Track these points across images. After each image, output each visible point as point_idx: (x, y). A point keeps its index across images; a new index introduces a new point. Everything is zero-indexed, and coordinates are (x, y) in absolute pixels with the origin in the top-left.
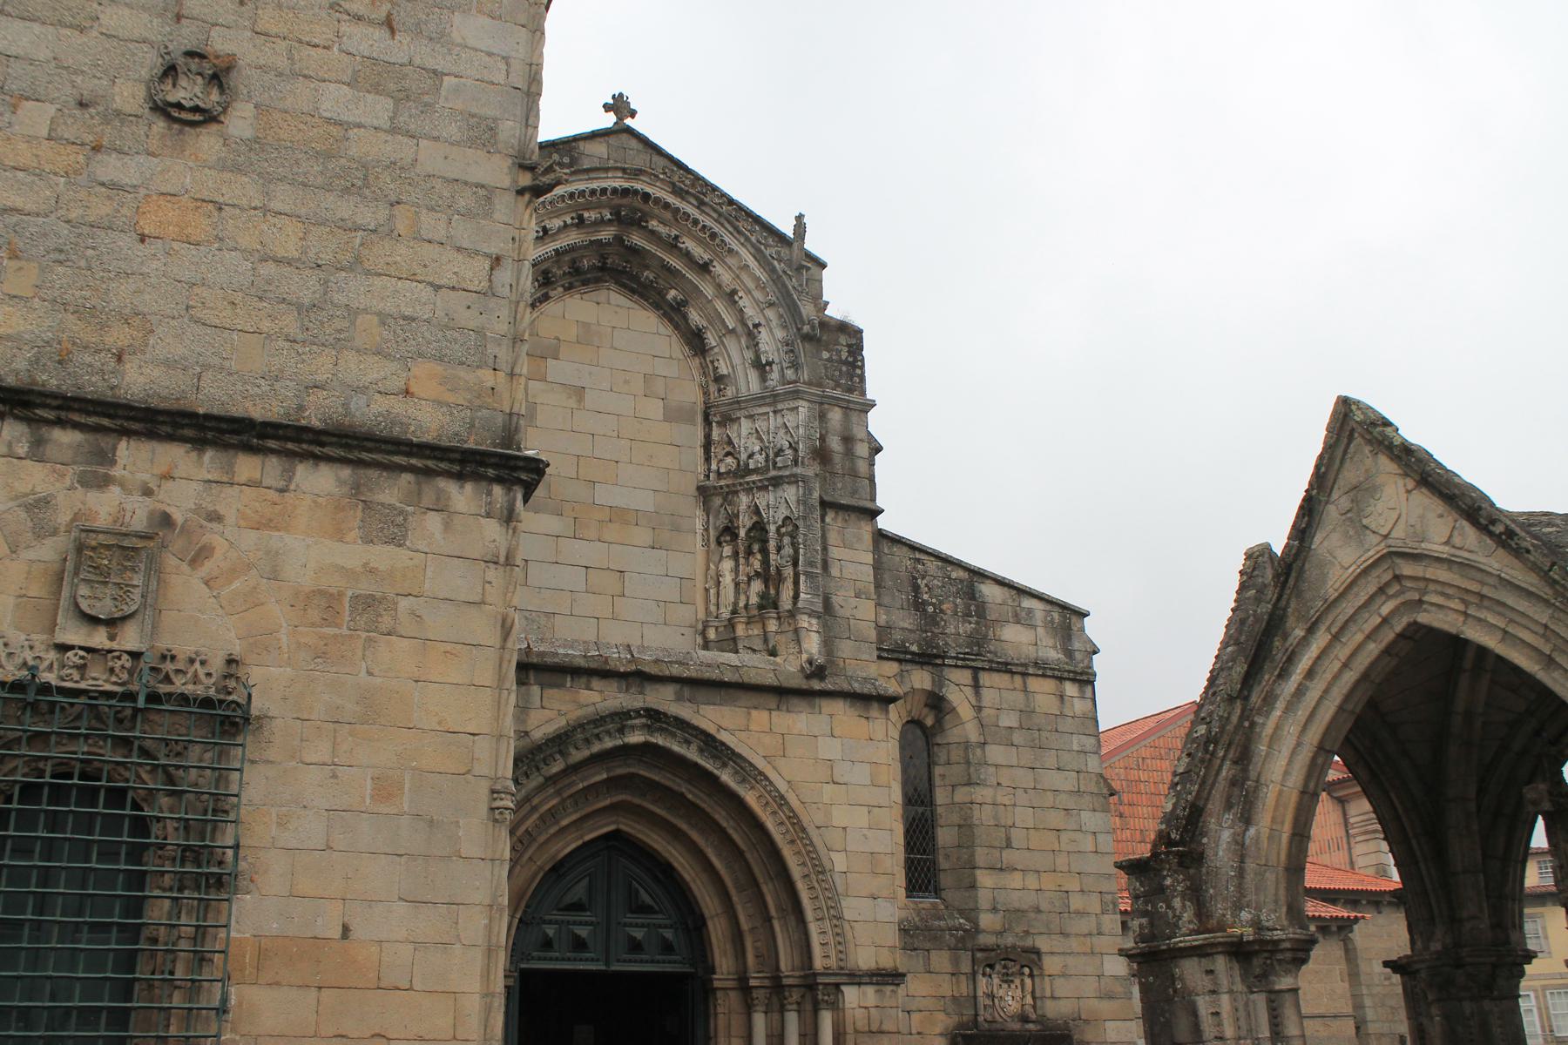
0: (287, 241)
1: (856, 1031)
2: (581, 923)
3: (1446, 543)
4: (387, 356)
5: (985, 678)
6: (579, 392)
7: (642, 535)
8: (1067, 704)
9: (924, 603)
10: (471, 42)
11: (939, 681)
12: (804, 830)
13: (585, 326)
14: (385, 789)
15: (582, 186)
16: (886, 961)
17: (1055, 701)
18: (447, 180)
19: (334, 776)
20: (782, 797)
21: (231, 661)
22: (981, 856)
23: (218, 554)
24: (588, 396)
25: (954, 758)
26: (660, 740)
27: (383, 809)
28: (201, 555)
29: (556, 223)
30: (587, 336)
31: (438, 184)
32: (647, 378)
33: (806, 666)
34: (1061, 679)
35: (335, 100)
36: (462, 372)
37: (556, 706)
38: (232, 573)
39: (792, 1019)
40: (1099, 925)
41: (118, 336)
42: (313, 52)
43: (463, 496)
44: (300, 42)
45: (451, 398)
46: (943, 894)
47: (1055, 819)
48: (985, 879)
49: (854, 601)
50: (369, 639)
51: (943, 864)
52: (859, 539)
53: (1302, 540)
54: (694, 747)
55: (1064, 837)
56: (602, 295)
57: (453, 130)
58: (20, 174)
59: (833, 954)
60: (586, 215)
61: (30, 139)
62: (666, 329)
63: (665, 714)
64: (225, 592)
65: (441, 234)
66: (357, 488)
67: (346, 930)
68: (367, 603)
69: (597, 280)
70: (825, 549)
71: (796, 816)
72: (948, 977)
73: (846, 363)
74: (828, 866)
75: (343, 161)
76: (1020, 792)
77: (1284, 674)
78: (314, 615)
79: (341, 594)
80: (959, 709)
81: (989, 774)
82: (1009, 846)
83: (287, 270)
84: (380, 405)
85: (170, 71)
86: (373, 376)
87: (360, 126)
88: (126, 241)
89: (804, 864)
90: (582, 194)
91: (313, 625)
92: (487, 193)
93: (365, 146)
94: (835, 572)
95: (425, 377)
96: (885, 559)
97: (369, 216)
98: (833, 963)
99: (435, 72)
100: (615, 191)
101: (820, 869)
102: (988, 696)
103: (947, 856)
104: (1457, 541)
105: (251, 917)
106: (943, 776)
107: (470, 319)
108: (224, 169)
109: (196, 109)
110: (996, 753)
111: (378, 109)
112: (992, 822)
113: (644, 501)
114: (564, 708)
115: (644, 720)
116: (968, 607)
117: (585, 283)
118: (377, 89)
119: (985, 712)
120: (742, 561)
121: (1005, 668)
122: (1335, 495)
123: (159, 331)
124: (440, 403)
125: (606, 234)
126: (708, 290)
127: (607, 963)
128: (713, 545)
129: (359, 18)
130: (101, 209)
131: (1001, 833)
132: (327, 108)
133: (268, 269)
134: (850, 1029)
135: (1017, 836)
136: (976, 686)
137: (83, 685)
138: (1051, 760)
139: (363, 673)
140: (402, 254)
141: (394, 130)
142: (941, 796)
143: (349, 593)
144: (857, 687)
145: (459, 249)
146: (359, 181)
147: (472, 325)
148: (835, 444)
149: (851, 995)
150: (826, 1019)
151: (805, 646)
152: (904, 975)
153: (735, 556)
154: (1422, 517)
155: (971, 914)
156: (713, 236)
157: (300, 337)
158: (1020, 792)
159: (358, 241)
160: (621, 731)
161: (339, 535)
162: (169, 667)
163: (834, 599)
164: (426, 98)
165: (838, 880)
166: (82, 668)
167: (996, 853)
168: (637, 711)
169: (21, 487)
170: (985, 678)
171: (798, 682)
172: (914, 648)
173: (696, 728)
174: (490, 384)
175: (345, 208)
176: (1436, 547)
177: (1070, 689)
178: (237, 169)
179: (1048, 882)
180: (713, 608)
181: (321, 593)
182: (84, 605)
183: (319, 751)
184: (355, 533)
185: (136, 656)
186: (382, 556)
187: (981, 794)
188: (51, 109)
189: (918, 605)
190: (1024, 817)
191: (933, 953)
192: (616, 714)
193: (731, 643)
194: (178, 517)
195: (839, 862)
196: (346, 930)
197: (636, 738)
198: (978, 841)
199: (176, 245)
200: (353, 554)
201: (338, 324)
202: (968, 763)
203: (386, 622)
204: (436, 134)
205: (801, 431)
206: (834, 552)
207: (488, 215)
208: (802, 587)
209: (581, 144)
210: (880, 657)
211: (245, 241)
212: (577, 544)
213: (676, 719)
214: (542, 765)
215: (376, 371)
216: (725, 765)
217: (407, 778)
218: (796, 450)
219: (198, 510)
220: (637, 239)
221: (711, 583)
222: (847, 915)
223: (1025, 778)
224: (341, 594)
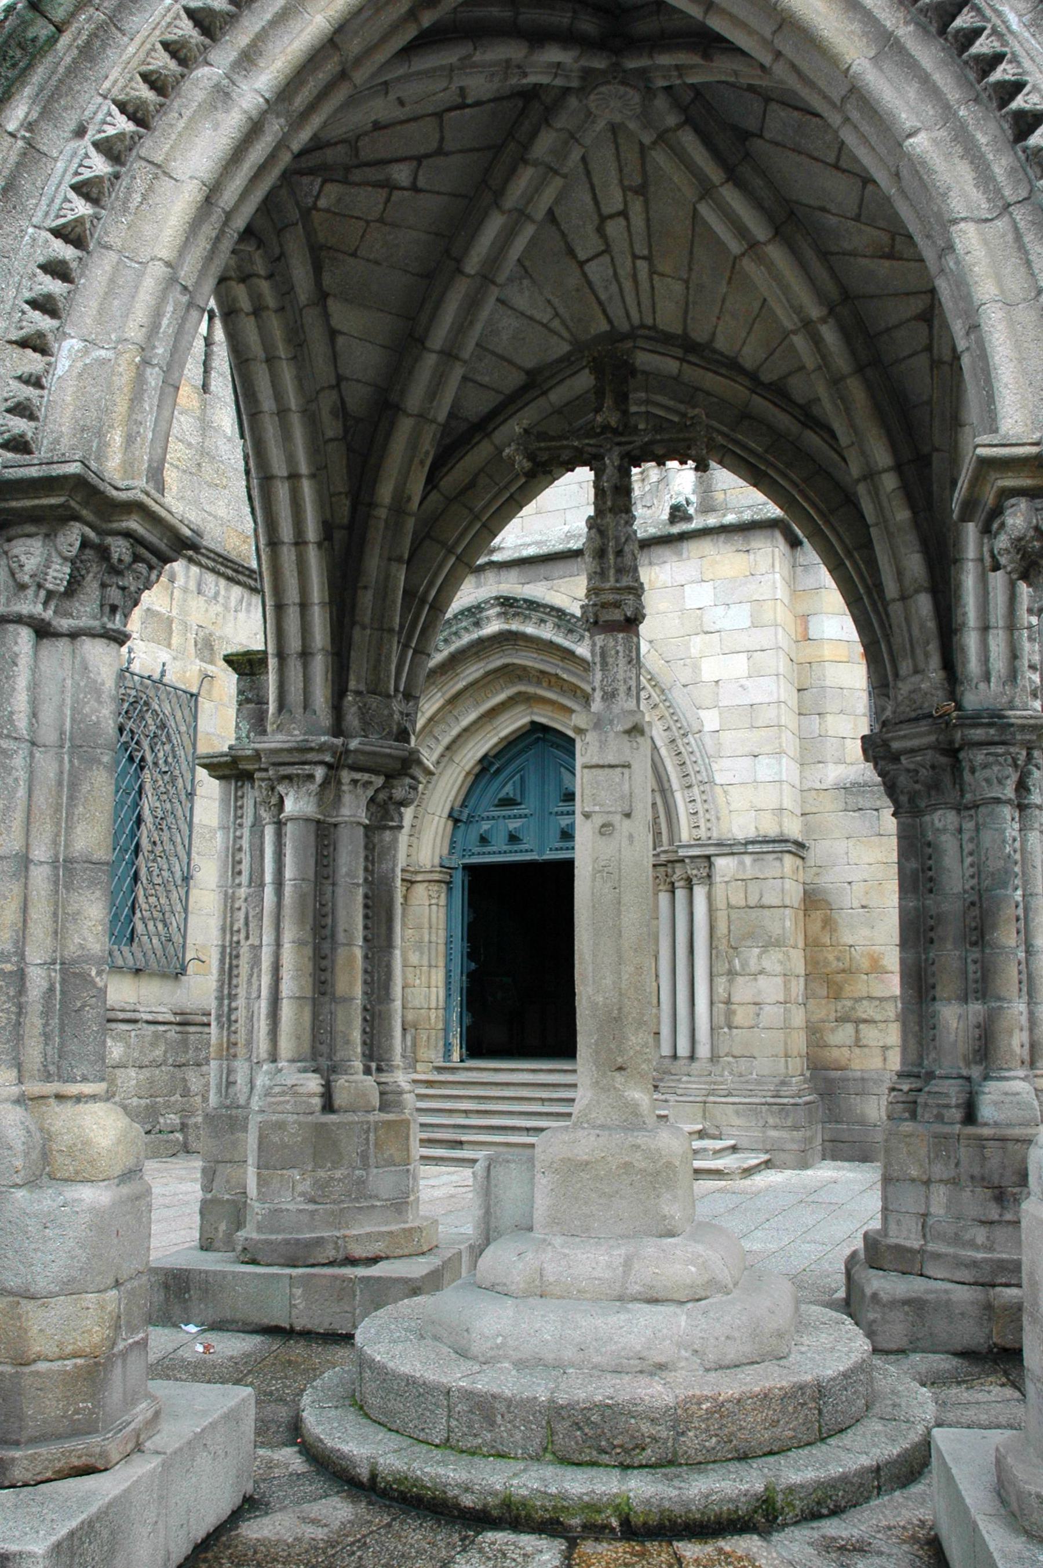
1: (729, 906)
12: (663, 691)
26: (515, 626)
39: (681, 894)
54: (550, 625)
63: (516, 600)
115: (498, 609)
127: (541, 853)
149: (724, 865)
150: (700, 893)
160: (477, 624)
165: (708, 740)
168: (486, 602)
173: (545, 606)
192: (469, 609)
195: (710, 720)
197: (493, 627)
213: (525, 601)
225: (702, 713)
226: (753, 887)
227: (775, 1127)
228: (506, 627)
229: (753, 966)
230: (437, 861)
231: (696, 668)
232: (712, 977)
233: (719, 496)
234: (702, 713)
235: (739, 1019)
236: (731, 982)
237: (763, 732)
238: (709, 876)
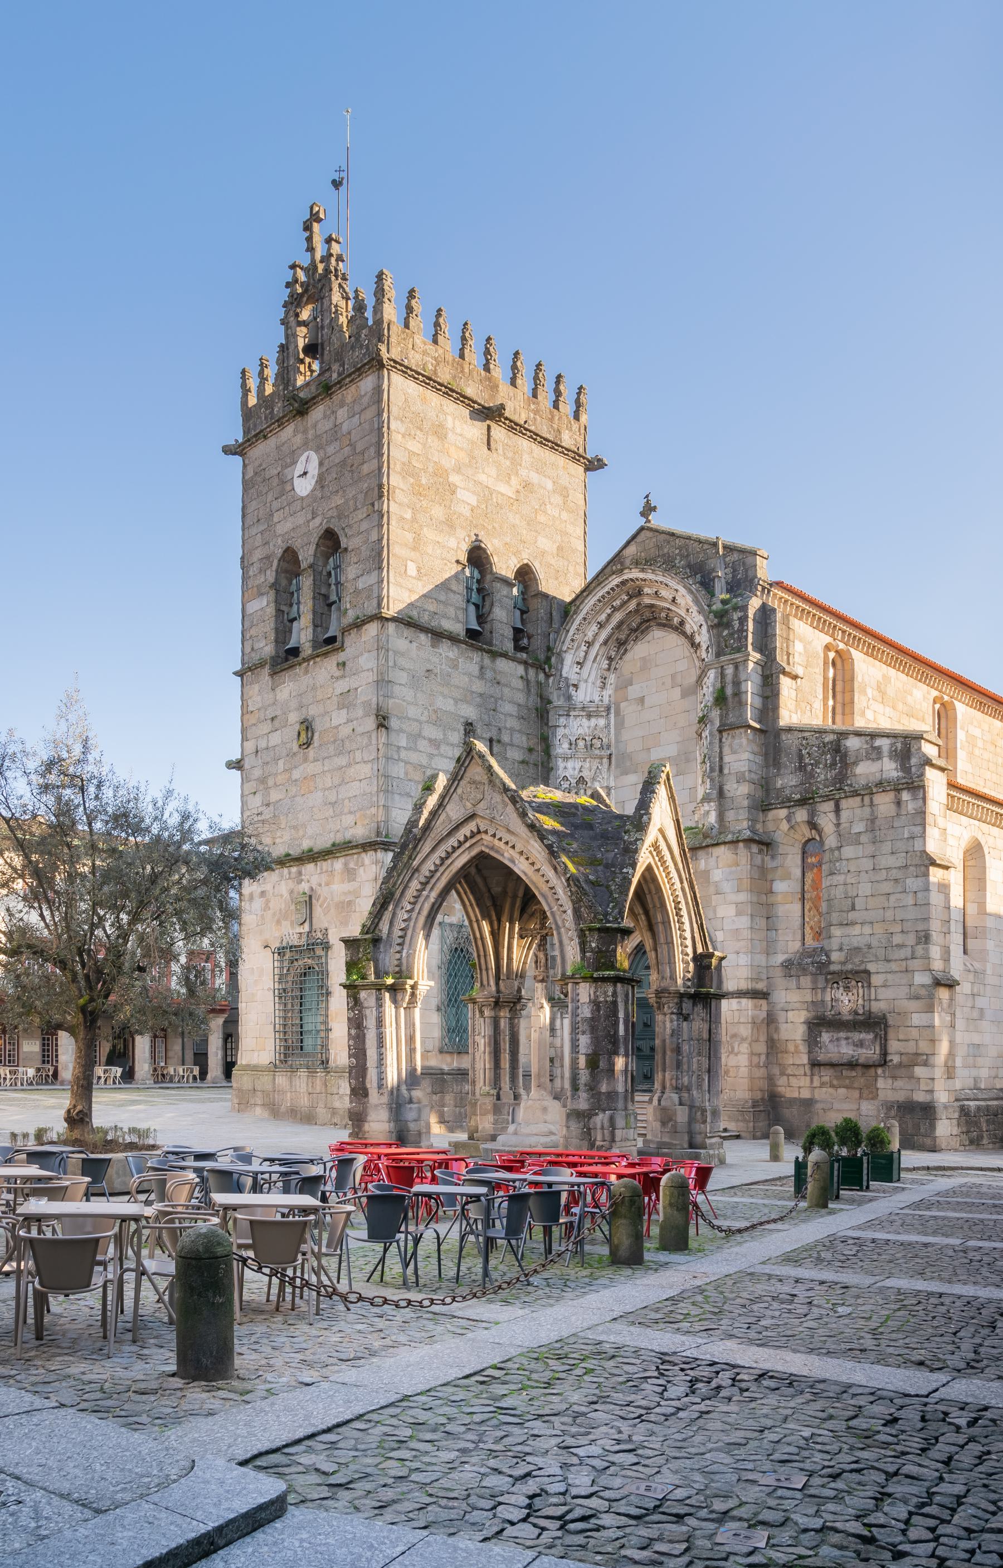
5: (844, 804)
6: (641, 700)
8: (903, 806)
11: (812, 814)
13: (643, 659)
15: (600, 594)
17: (893, 807)
29: (603, 617)
30: (646, 664)
32: (673, 676)
40: (913, 952)
47: (886, 887)
48: (837, 932)
52: (741, 746)
55: (892, 898)
56: (649, 637)
62: (681, 640)
69: (647, 628)
82: (853, 908)
90: (603, 597)
95: (348, 820)
97: (342, 761)
102: (844, 815)
107: (368, 790)
116: (834, 759)
117: (642, 632)
121: (855, 794)
125: (632, 605)
131: (849, 902)
132: (335, 722)
135: (859, 903)
138: (887, 847)
140: (351, 771)
148: (729, 691)
158: (863, 874)
167: (845, 915)
179: (879, 929)
190: (865, 889)
220: (647, 601)
223: (867, 864)
237: (743, 943)
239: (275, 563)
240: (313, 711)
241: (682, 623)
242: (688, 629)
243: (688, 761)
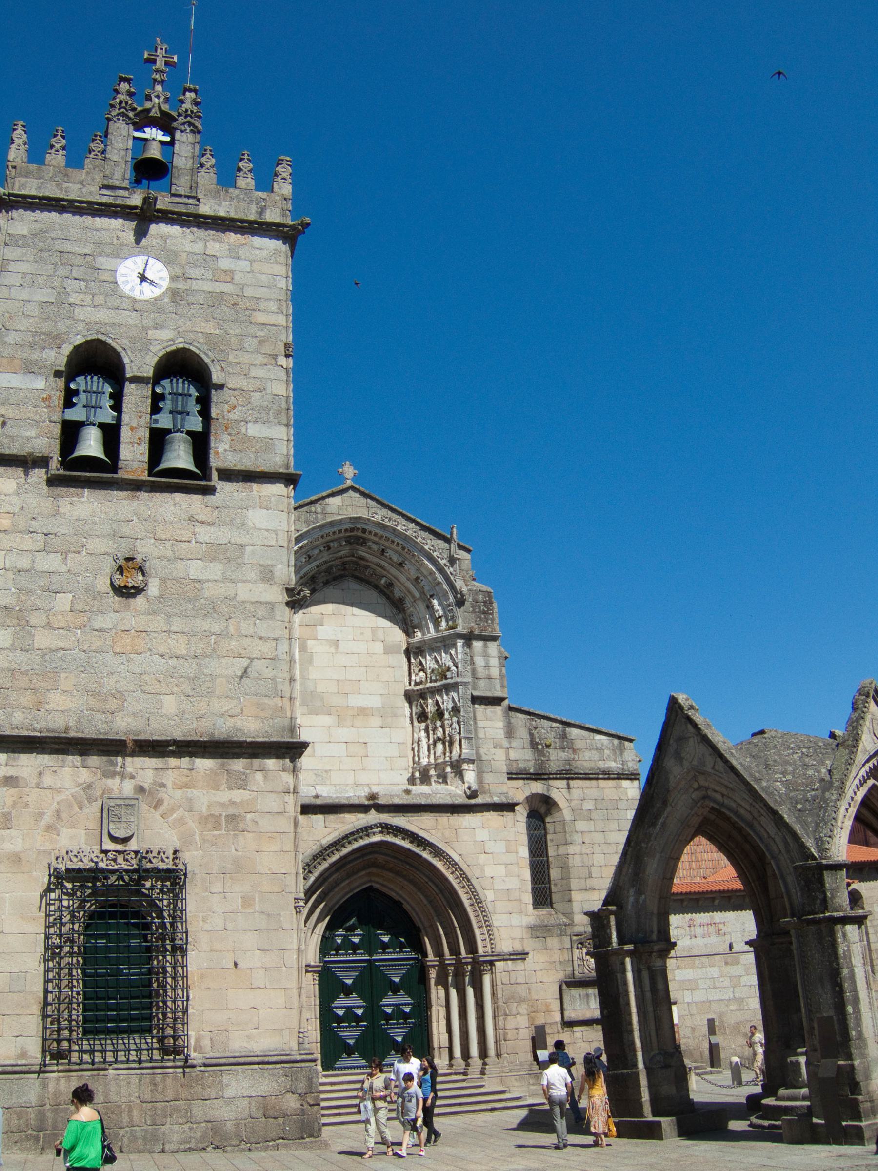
0: (180, 645)
2: (355, 935)
3: (713, 768)
4: (232, 698)
6: (336, 643)
7: (376, 721)
9: (537, 744)
10: (258, 526)
12: (469, 880)
14: (247, 901)
16: (518, 948)
18: (252, 603)
19: (225, 898)
20: (456, 864)
21: (175, 852)
22: (574, 884)
23: (166, 803)
24: (342, 644)
25: (557, 830)
26: (390, 838)
27: (247, 910)
28: (158, 804)
29: (316, 552)
31: (248, 606)
33: (467, 791)
34: (618, 779)
35: (196, 569)
36: (266, 700)
37: (333, 825)
38: (173, 810)
41: (113, 704)
42: (183, 545)
43: (271, 763)
44: (176, 540)
45: (262, 714)
46: (554, 905)
48: (576, 896)
49: (493, 751)
50: (235, 835)
51: (553, 889)
53: (658, 763)
57: (253, 575)
58: (61, 631)
59: (489, 945)
60: (332, 544)
61: (62, 613)
64: (171, 819)
65: (251, 631)
66: (223, 765)
67: (236, 964)
68: (232, 819)
69: (341, 577)
70: (475, 723)
71: (464, 873)
72: (556, 951)
73: (484, 612)
74: (483, 898)
75: (202, 601)
76: (596, 846)
77: (654, 825)
78: (210, 826)
79: (220, 815)
80: (559, 803)
81: (577, 838)
82: (590, 876)
83: (181, 661)
84: (231, 722)
85: (120, 570)
86: (225, 708)
87: (208, 581)
88: (109, 657)
89: (470, 898)
91: (210, 830)
92: (271, 606)
93: (211, 591)
94: (481, 734)
96: (512, 720)
98: (489, 949)
99: (241, 545)
100: (346, 530)
101: (478, 901)
102: (576, 793)
103: (555, 885)
104: (716, 767)
105: (196, 960)
106: (552, 840)
108: (149, 613)
109: (133, 587)
110: (581, 825)
111: (216, 570)
112: (580, 864)
113: (375, 702)
114: (337, 827)
117: (335, 579)
118: (213, 560)
119: (573, 804)
120: (431, 732)
121: (586, 777)
122: (671, 741)
123: (129, 699)
124: (256, 717)
126: (403, 578)
128: (416, 723)
129: (202, 522)
130: (97, 643)
133: (173, 662)
134: (499, 983)
135: (595, 871)
136: (569, 788)
137: (116, 867)
139: (233, 850)
141: (225, 579)
142: (551, 852)
143: (224, 814)
144: (496, 799)
145: (261, 638)
146: (211, 609)
147: (270, 676)
151: (466, 779)
152: (527, 954)
153: (427, 730)
154: (703, 755)
155: (569, 915)
156: (403, 548)
157: (191, 694)
158: (596, 846)
159: (213, 641)
161: (217, 788)
162: (150, 856)
163: (482, 751)
164: (239, 561)
165: (489, 905)
166: (115, 860)
167: (583, 881)
168: (375, 825)
169: (81, 780)
170: (573, 783)
171: (462, 800)
172: (532, 771)
174: (280, 705)
175: (206, 625)
176: (709, 769)
177: (626, 783)
178: (154, 613)
180: (416, 759)
181: (212, 815)
182: (112, 832)
183: (217, 887)
184: (224, 786)
185: (136, 853)
186: (238, 795)
187: (571, 849)
188: (70, 596)
189: (534, 745)
191: (548, 939)
192: (365, 828)
193: (425, 778)
194: (146, 786)
195: (488, 896)
196: (236, 964)
198: (572, 876)
199: (132, 656)
200: (225, 795)
201: (207, 685)
202: (565, 832)
203: (241, 826)
204: (245, 579)
205: (459, 657)
206: (480, 724)
207: (272, 618)
208: (463, 746)
209: (327, 500)
210: (509, 779)
211: (162, 650)
212: (340, 730)
214: (327, 857)
215: (227, 706)
216: (424, 850)
217: (257, 895)
218: (457, 667)
219: (155, 783)
221: (415, 745)
222: (496, 923)
223: (598, 838)
224: (220, 815)
225: (487, 892)
226: (512, 974)
227: (533, 1084)
228: (384, 839)
229: (514, 1011)
230: (317, 960)
231: (482, 870)
232: (494, 1017)
233: (487, 786)
234: (487, 892)
235: (509, 1037)
236: (505, 1020)
238: (491, 969)
239: (67, 349)
240: (144, 549)
241: (390, 585)
242: (397, 594)
243: (395, 715)
